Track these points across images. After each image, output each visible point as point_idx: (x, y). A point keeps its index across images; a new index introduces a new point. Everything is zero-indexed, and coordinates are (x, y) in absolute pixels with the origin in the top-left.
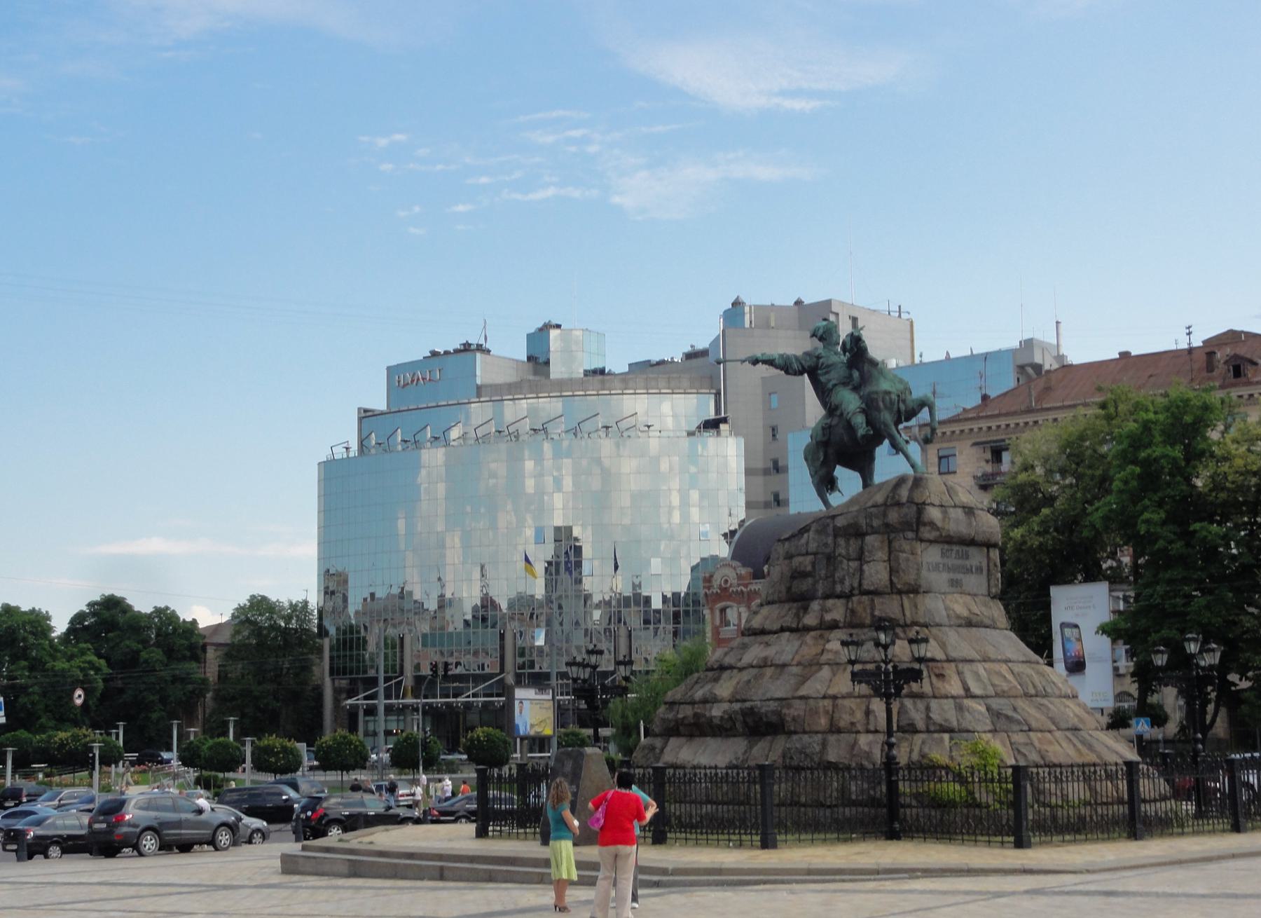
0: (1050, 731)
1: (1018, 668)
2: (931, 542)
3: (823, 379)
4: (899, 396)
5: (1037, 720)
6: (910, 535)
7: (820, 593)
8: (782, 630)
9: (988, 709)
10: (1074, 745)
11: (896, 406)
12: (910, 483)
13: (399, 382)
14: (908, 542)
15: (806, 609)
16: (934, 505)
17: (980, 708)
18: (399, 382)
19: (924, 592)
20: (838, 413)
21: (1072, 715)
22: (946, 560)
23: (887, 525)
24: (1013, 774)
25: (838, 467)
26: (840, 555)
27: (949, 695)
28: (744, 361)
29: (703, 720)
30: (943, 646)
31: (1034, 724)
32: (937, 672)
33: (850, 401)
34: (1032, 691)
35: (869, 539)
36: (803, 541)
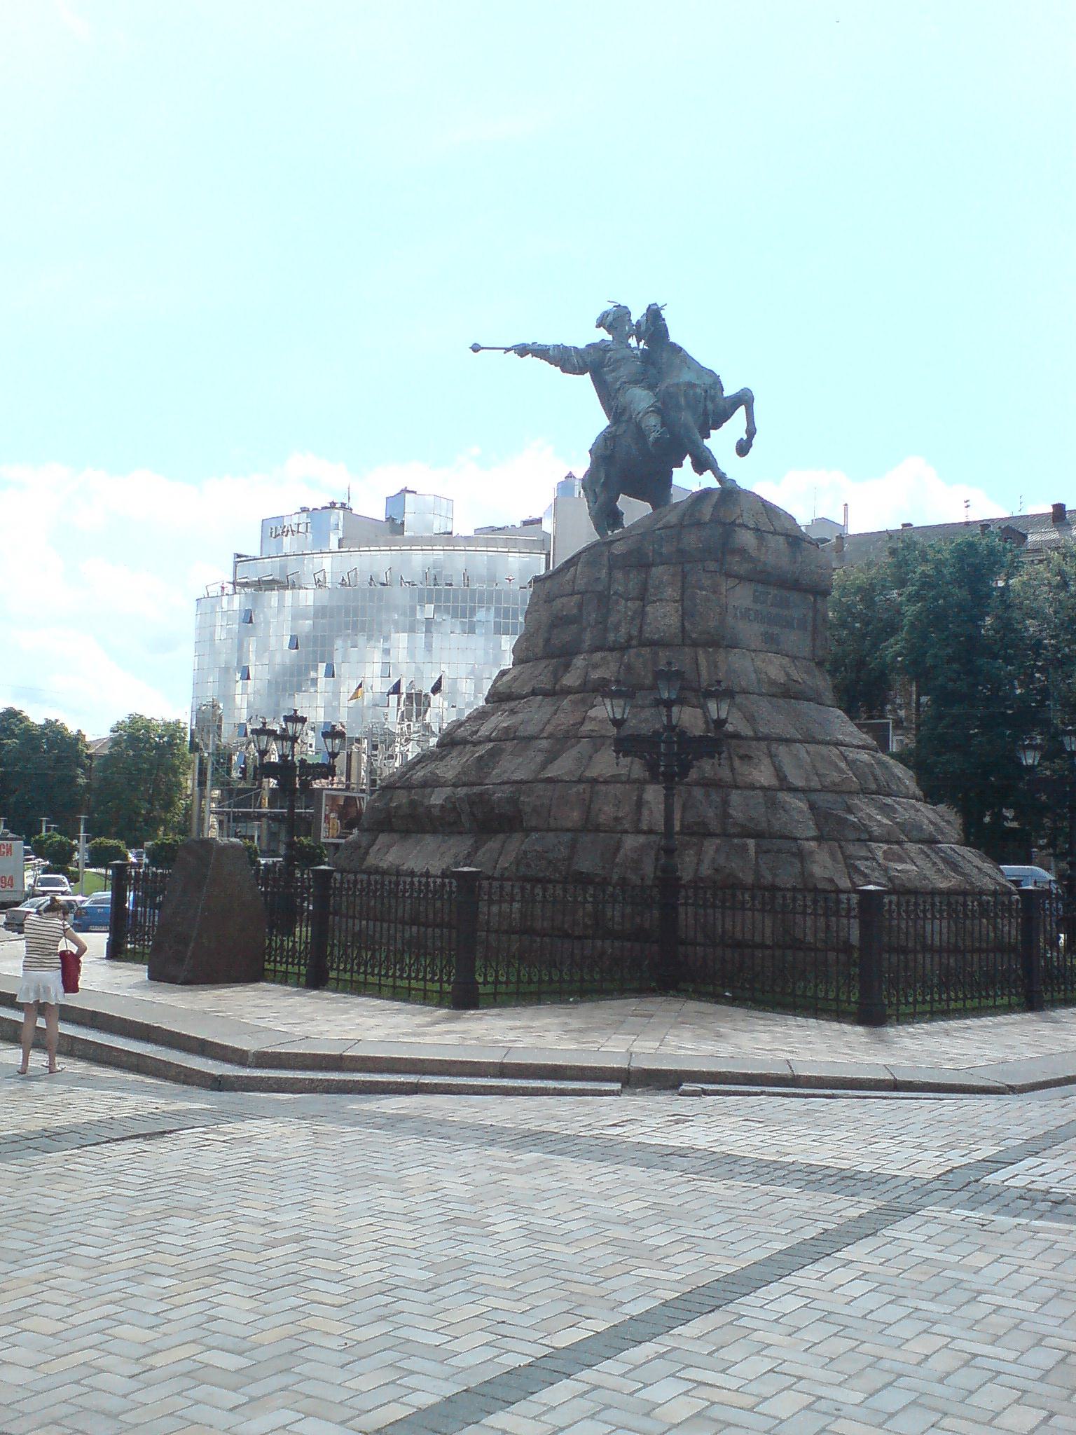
0: (899, 843)
1: (852, 754)
2: (741, 578)
3: (609, 378)
4: (706, 392)
5: (880, 824)
6: (712, 566)
7: (586, 646)
8: (534, 693)
9: (812, 807)
10: (934, 864)
11: (701, 405)
12: (715, 497)
13: (271, 533)
14: (709, 575)
15: (567, 666)
16: (747, 527)
17: (801, 804)
18: (271, 533)
19: (727, 646)
20: (625, 418)
21: (926, 822)
22: (758, 607)
23: (681, 552)
24: (860, 903)
25: (621, 496)
26: (615, 593)
27: (758, 785)
28: (508, 350)
29: (421, 810)
30: (750, 719)
31: (877, 831)
32: (742, 752)
33: (641, 399)
34: (874, 787)
35: (655, 571)
36: (569, 576)
